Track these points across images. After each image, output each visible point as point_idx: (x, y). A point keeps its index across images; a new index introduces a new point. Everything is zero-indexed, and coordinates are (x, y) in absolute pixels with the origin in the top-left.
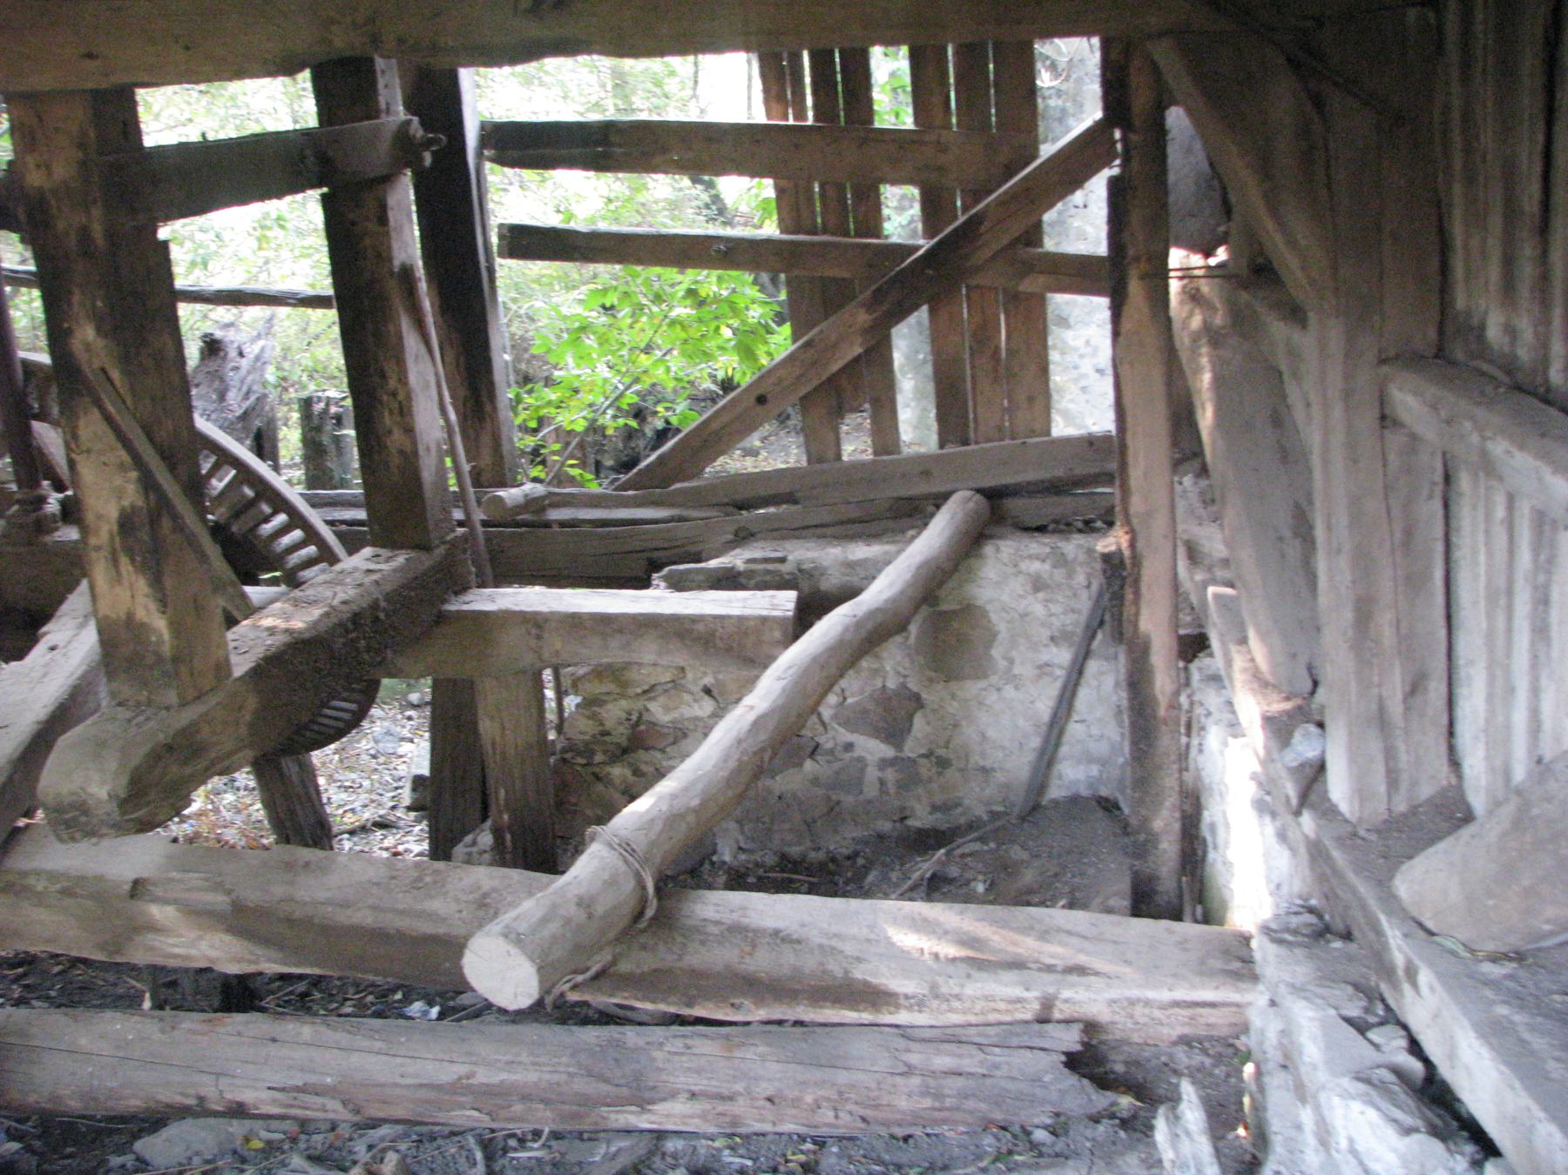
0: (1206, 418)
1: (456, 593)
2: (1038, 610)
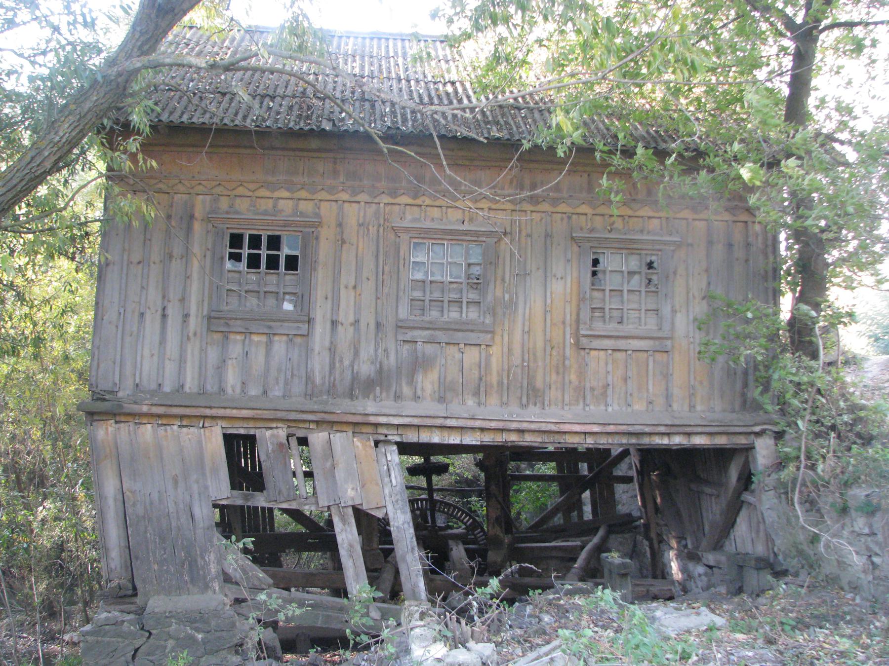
0: (659, 500)
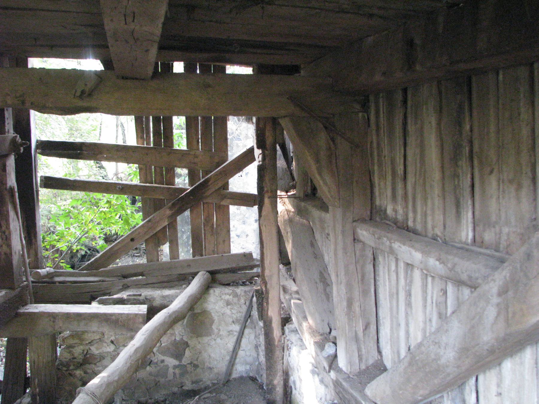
1: (23, 306)
2: (228, 312)
